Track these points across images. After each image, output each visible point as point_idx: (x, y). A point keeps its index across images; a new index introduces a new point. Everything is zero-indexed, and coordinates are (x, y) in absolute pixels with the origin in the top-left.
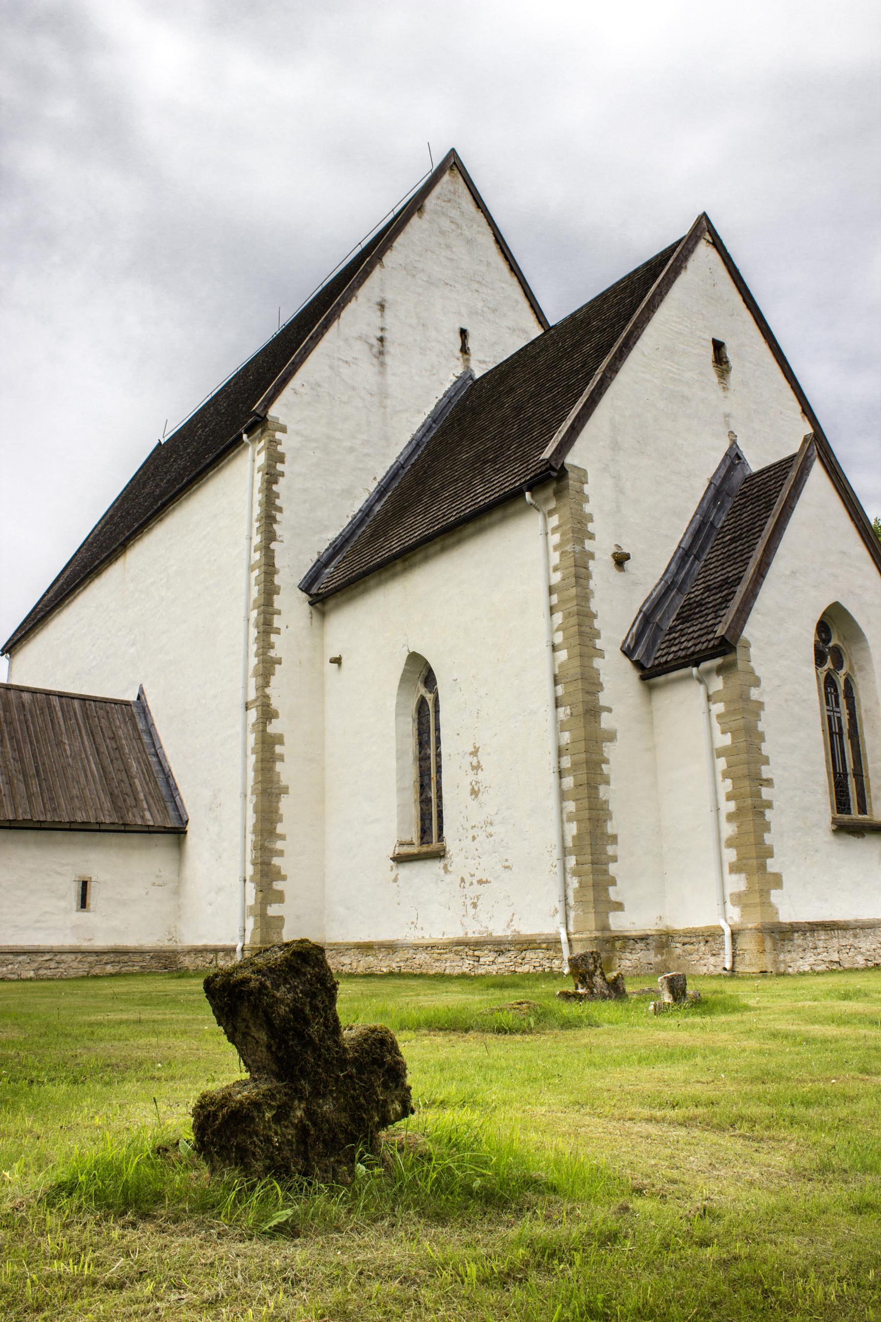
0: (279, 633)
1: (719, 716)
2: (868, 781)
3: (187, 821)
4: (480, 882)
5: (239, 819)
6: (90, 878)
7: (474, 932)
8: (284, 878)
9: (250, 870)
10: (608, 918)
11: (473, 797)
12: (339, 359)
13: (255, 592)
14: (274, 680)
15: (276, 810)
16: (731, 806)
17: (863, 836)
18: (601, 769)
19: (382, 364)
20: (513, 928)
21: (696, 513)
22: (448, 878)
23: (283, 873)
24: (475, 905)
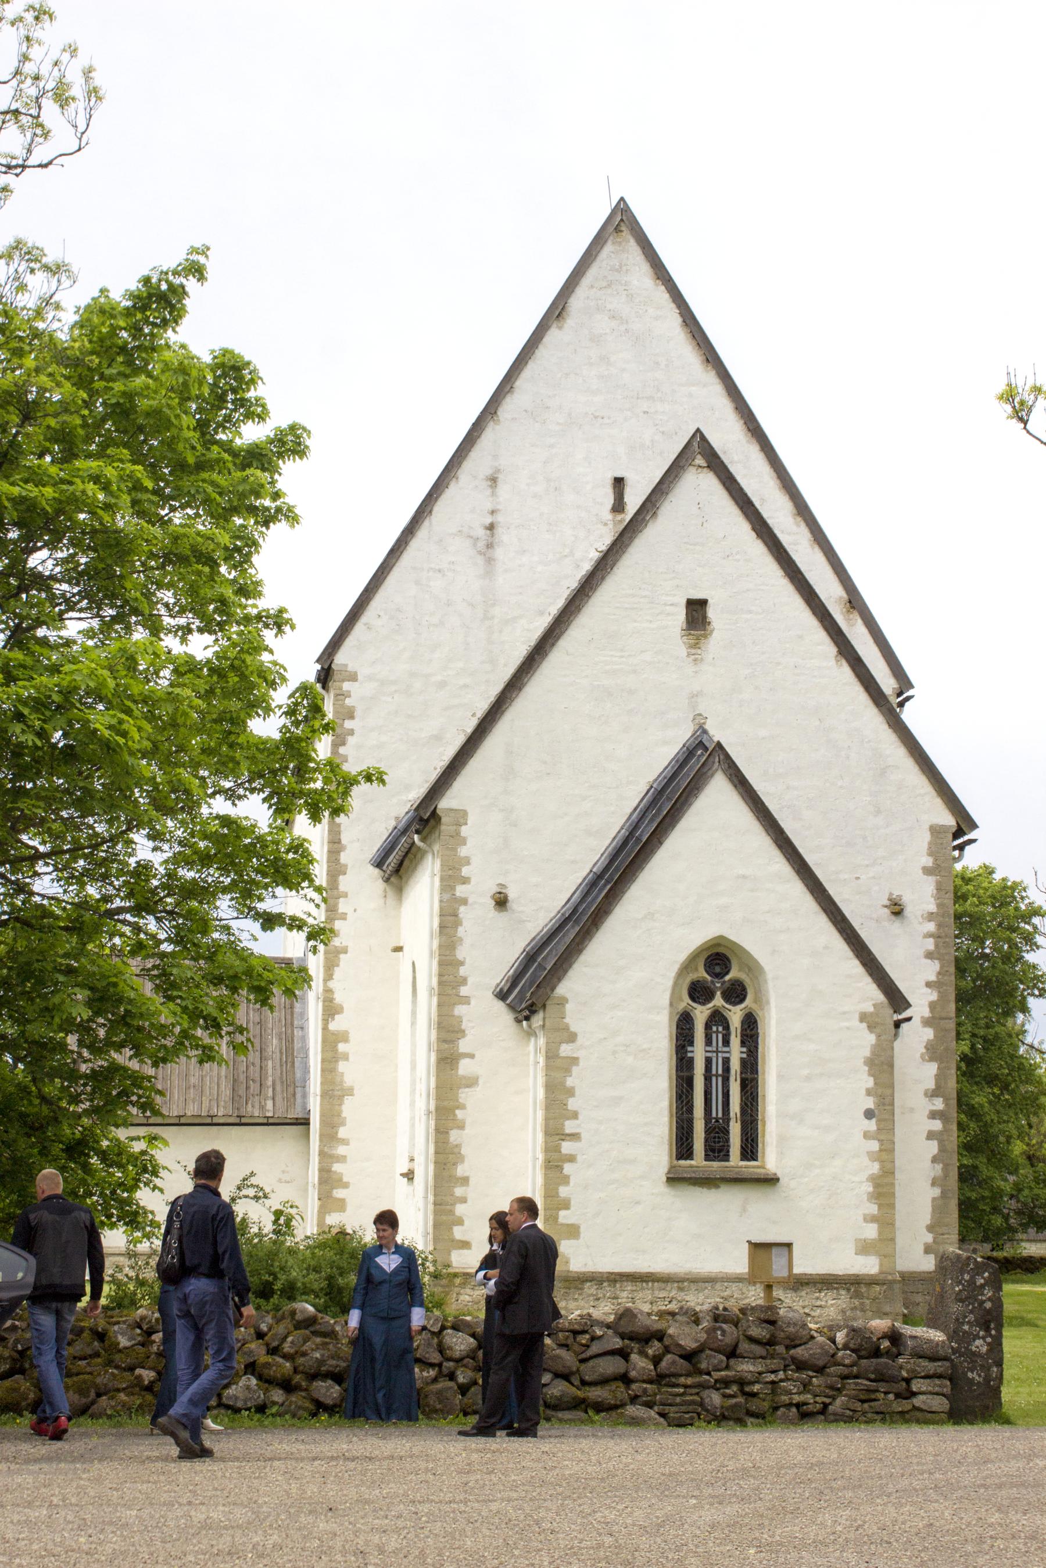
0: (345, 919)
8: (346, 1186)
10: (449, 1255)
12: (430, 569)
14: (338, 973)
17: (717, 1187)
18: (455, 1115)
19: (490, 561)
21: (622, 828)
23: (345, 1179)
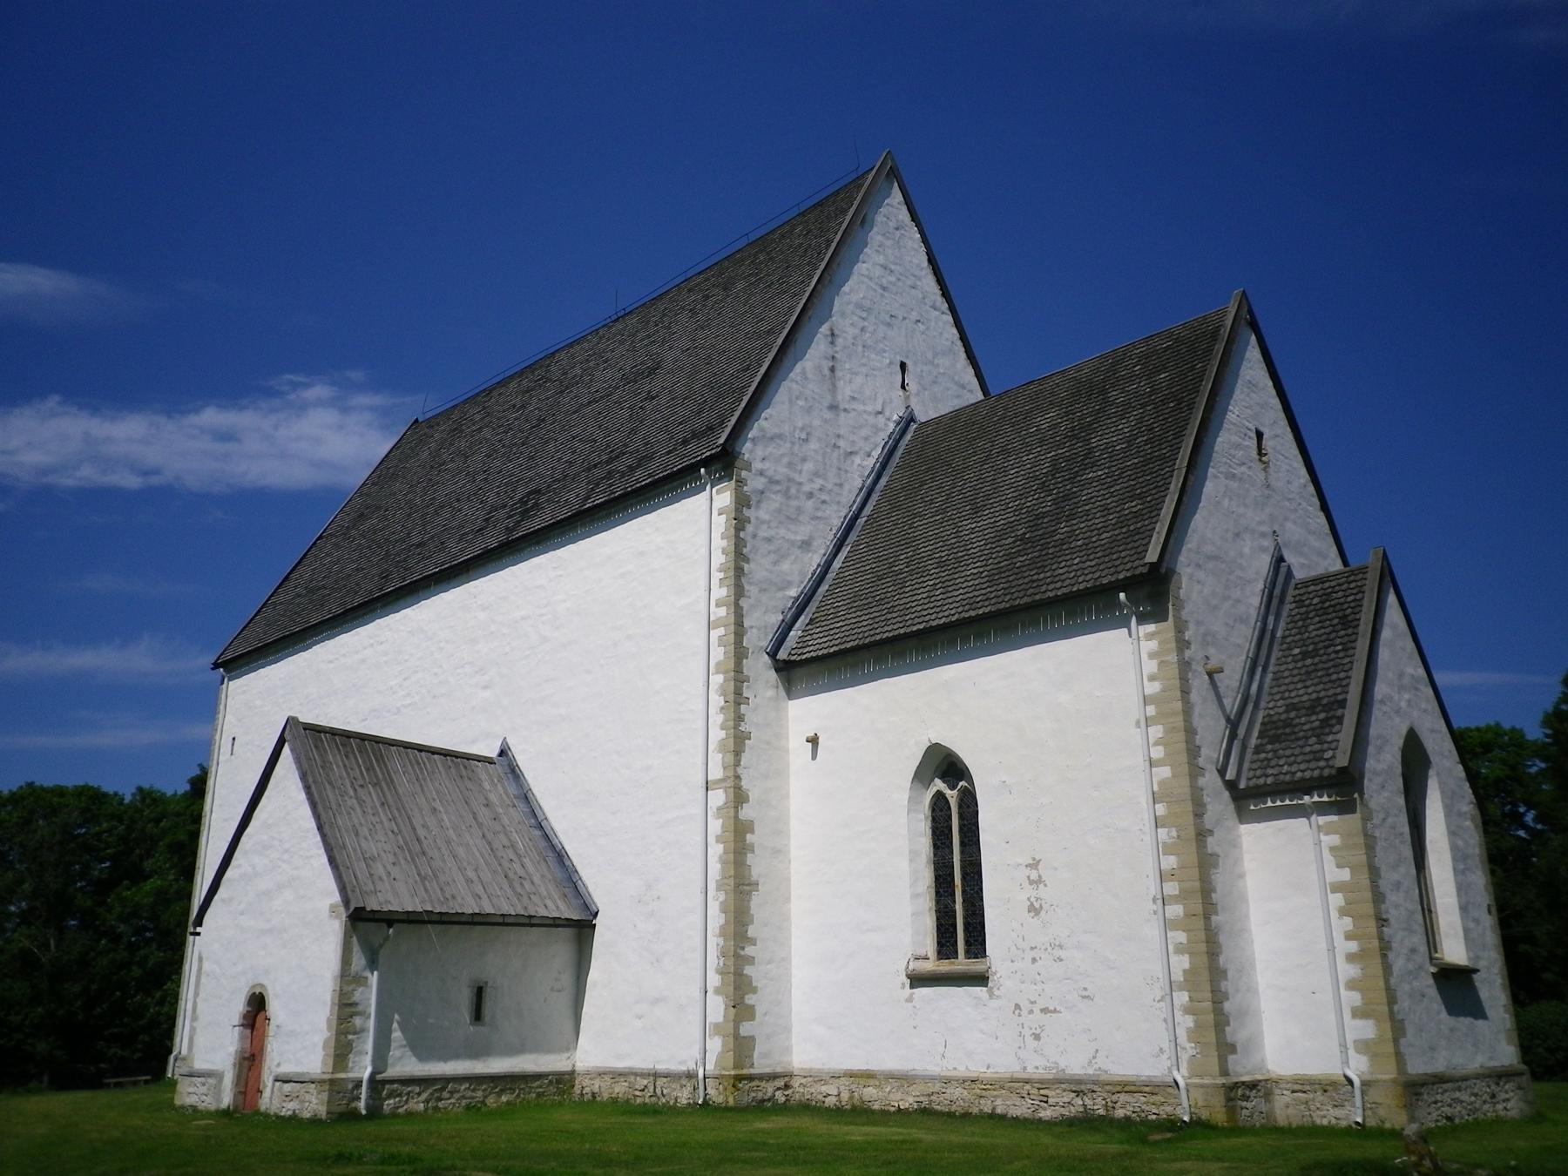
1: (1332, 849)
2: (1437, 918)
3: (597, 913)
4: (1045, 1011)
5: (697, 919)
6: (486, 983)
7: (1037, 1068)
9: (714, 980)
11: (1032, 914)
13: (718, 654)
15: (749, 908)
16: (1353, 946)
20: (1097, 1066)
22: (994, 1003)
24: (1037, 1037)
